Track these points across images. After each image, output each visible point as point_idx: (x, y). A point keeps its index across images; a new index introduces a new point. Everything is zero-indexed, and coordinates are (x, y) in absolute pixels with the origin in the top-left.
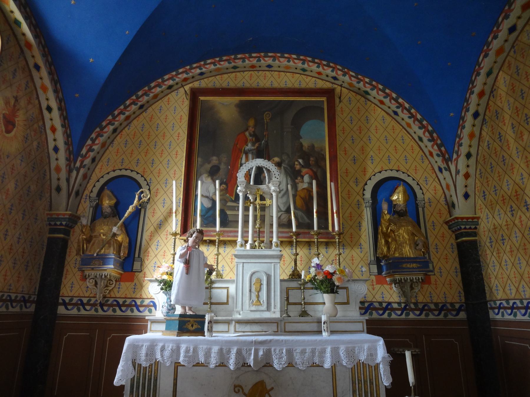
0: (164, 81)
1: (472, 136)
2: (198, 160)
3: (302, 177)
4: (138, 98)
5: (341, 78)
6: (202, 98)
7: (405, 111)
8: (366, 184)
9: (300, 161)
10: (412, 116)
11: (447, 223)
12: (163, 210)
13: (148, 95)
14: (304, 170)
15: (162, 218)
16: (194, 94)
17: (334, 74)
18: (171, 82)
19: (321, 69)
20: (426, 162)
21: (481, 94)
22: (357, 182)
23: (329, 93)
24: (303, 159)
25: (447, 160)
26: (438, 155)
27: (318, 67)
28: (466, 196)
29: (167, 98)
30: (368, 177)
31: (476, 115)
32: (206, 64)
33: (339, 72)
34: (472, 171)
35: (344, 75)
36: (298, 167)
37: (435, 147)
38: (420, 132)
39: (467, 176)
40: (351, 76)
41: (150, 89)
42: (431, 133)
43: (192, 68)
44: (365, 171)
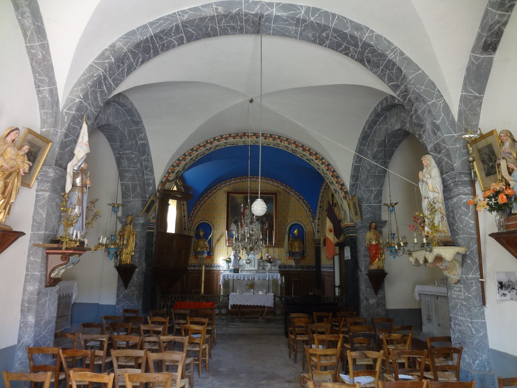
0: (217, 187)
1: (320, 213)
2: (230, 218)
3: (266, 224)
4: (208, 194)
5: (280, 187)
6: (231, 195)
7: (302, 200)
8: (287, 226)
9: (265, 218)
10: (304, 202)
11: (313, 240)
12: (219, 235)
13: (211, 193)
14: (266, 222)
15: (219, 238)
16: (228, 193)
17: (278, 185)
18: (219, 188)
19: (273, 183)
20: (308, 218)
21: (321, 202)
22: (284, 225)
23: (275, 194)
24: (265, 217)
25: (314, 219)
26: (311, 217)
27: (272, 182)
28: (318, 232)
29: (217, 192)
30: (288, 223)
31: (320, 207)
32: (231, 180)
33: (280, 185)
34: (320, 224)
35: (281, 186)
36: (264, 221)
37: (311, 214)
38: (306, 208)
39: (318, 225)
40: (284, 186)
41: (212, 190)
42: (309, 209)
43: (226, 182)
44: (287, 221)
